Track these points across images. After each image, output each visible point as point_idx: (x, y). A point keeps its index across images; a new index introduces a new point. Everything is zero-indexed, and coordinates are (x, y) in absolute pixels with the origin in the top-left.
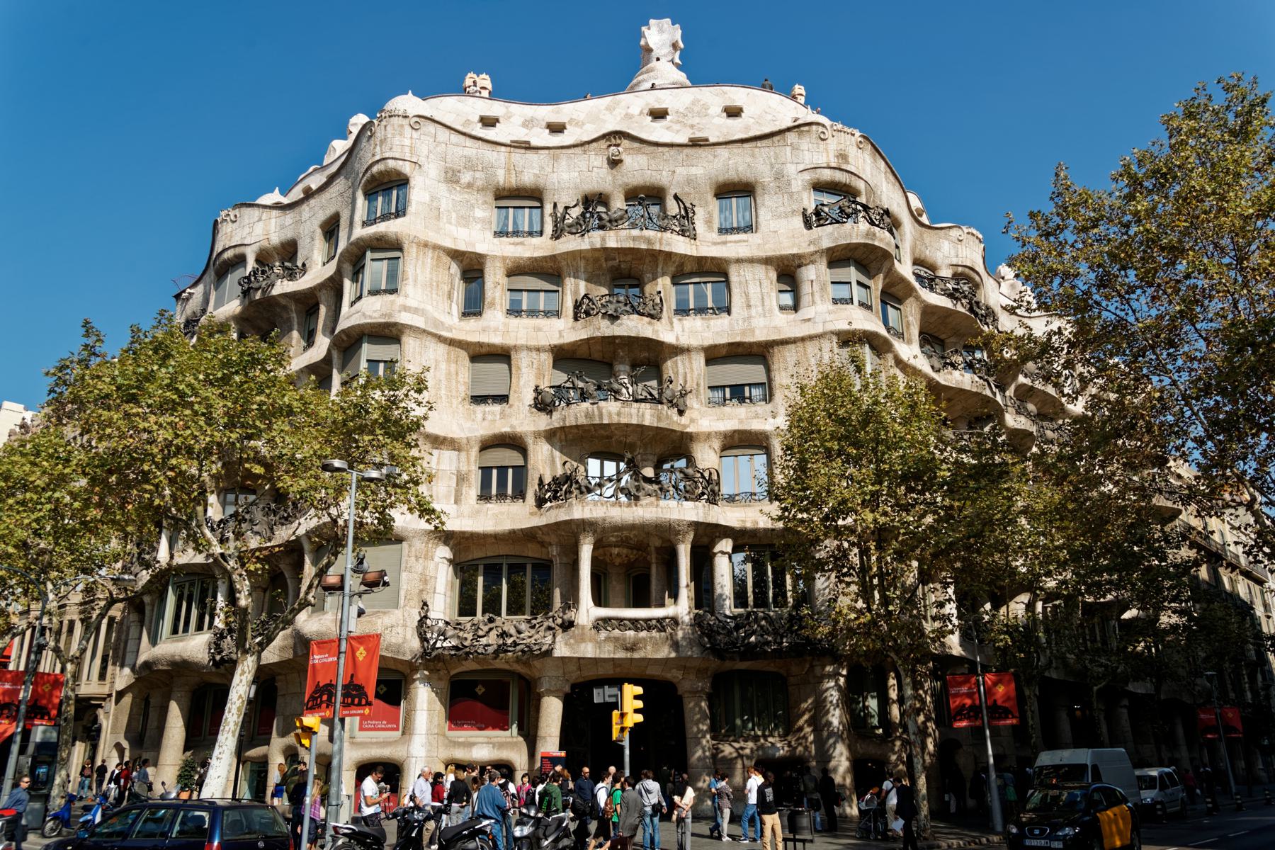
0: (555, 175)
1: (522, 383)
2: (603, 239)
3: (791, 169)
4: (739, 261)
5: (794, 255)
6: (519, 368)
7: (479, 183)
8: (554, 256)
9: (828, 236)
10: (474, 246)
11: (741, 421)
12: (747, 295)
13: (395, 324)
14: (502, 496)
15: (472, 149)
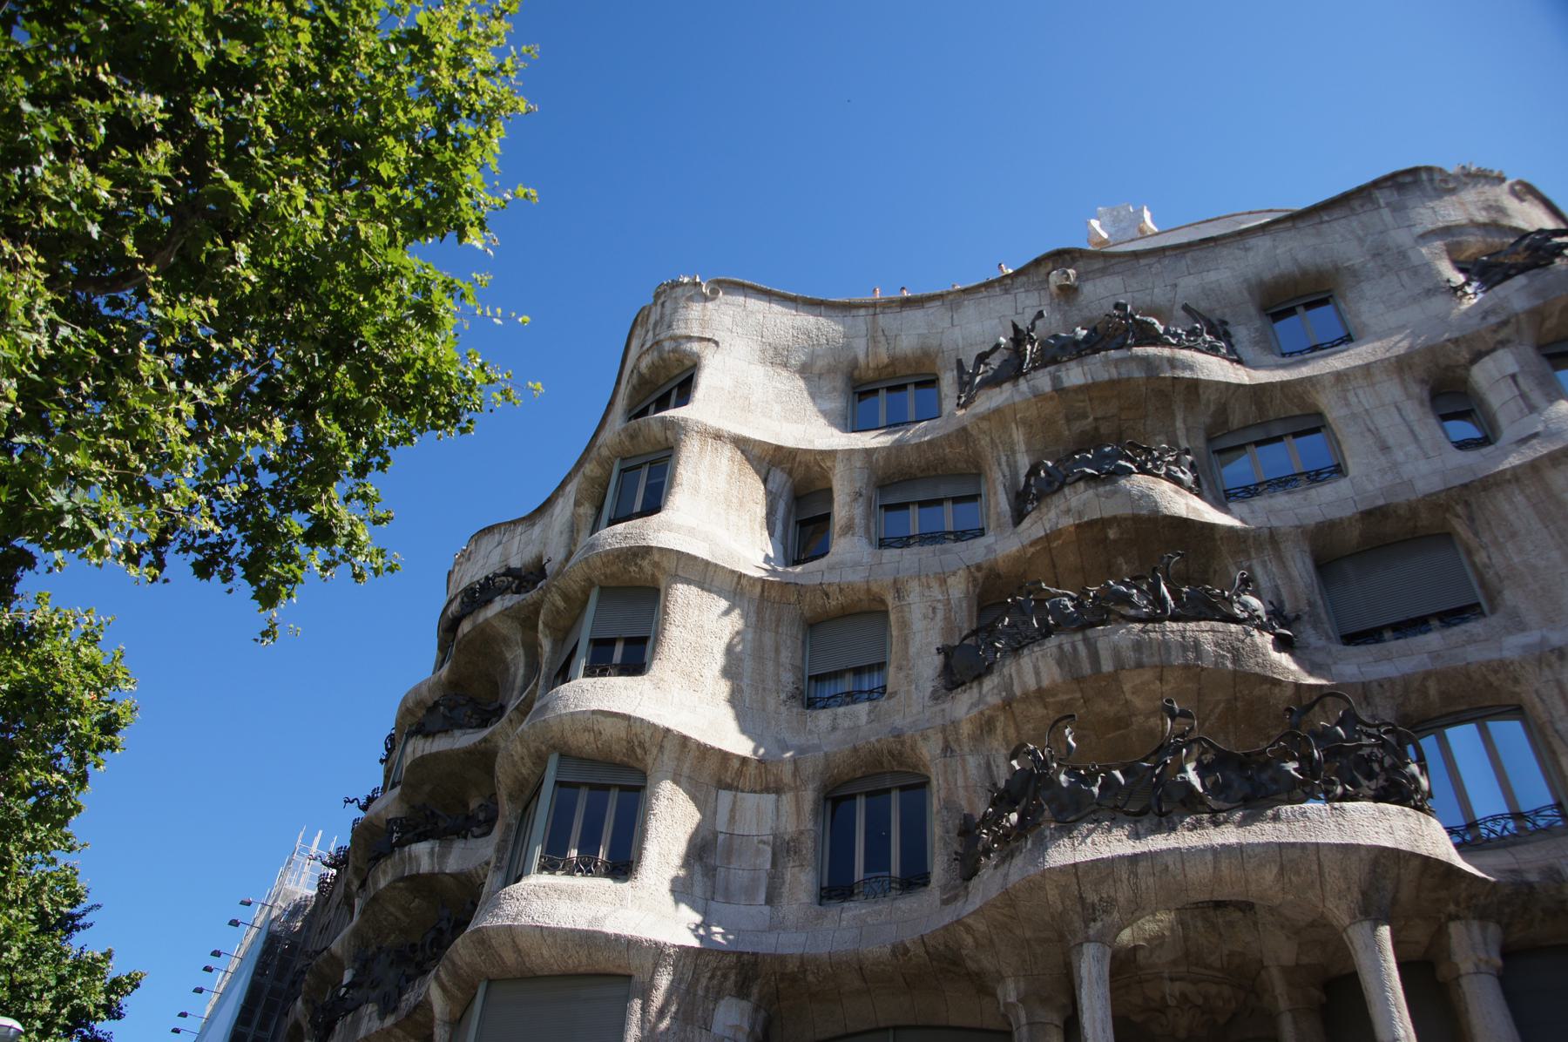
0: (957, 330)
1: (912, 650)
2: (1056, 380)
3: (1402, 237)
4: (1340, 377)
5: (1456, 341)
6: (904, 624)
7: (821, 363)
8: (964, 429)
9: (1516, 294)
10: (811, 442)
11: (1435, 656)
12: (1374, 432)
13: (648, 550)
14: (879, 887)
15: (808, 320)
